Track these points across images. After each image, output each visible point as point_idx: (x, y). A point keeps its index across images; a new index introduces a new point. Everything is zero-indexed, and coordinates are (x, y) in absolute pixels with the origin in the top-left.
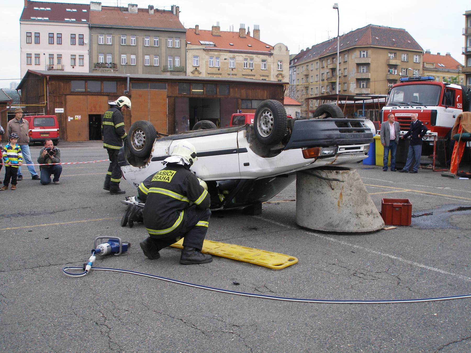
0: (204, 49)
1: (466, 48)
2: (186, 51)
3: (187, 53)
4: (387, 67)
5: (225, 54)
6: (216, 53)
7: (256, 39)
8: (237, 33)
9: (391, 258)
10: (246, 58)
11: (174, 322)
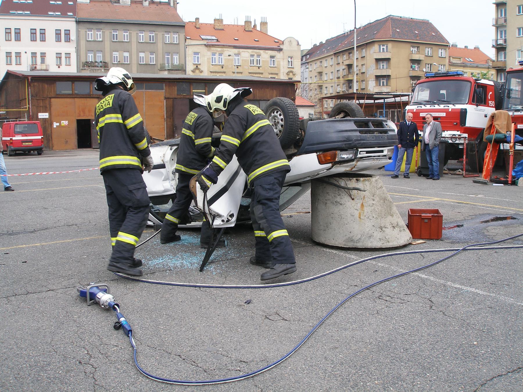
0: (205, 45)
1: (497, 41)
2: (186, 47)
3: (187, 50)
4: (409, 62)
5: (229, 49)
6: (219, 49)
7: (264, 33)
8: (242, 26)
9: (421, 278)
10: (253, 54)
11: (171, 359)
